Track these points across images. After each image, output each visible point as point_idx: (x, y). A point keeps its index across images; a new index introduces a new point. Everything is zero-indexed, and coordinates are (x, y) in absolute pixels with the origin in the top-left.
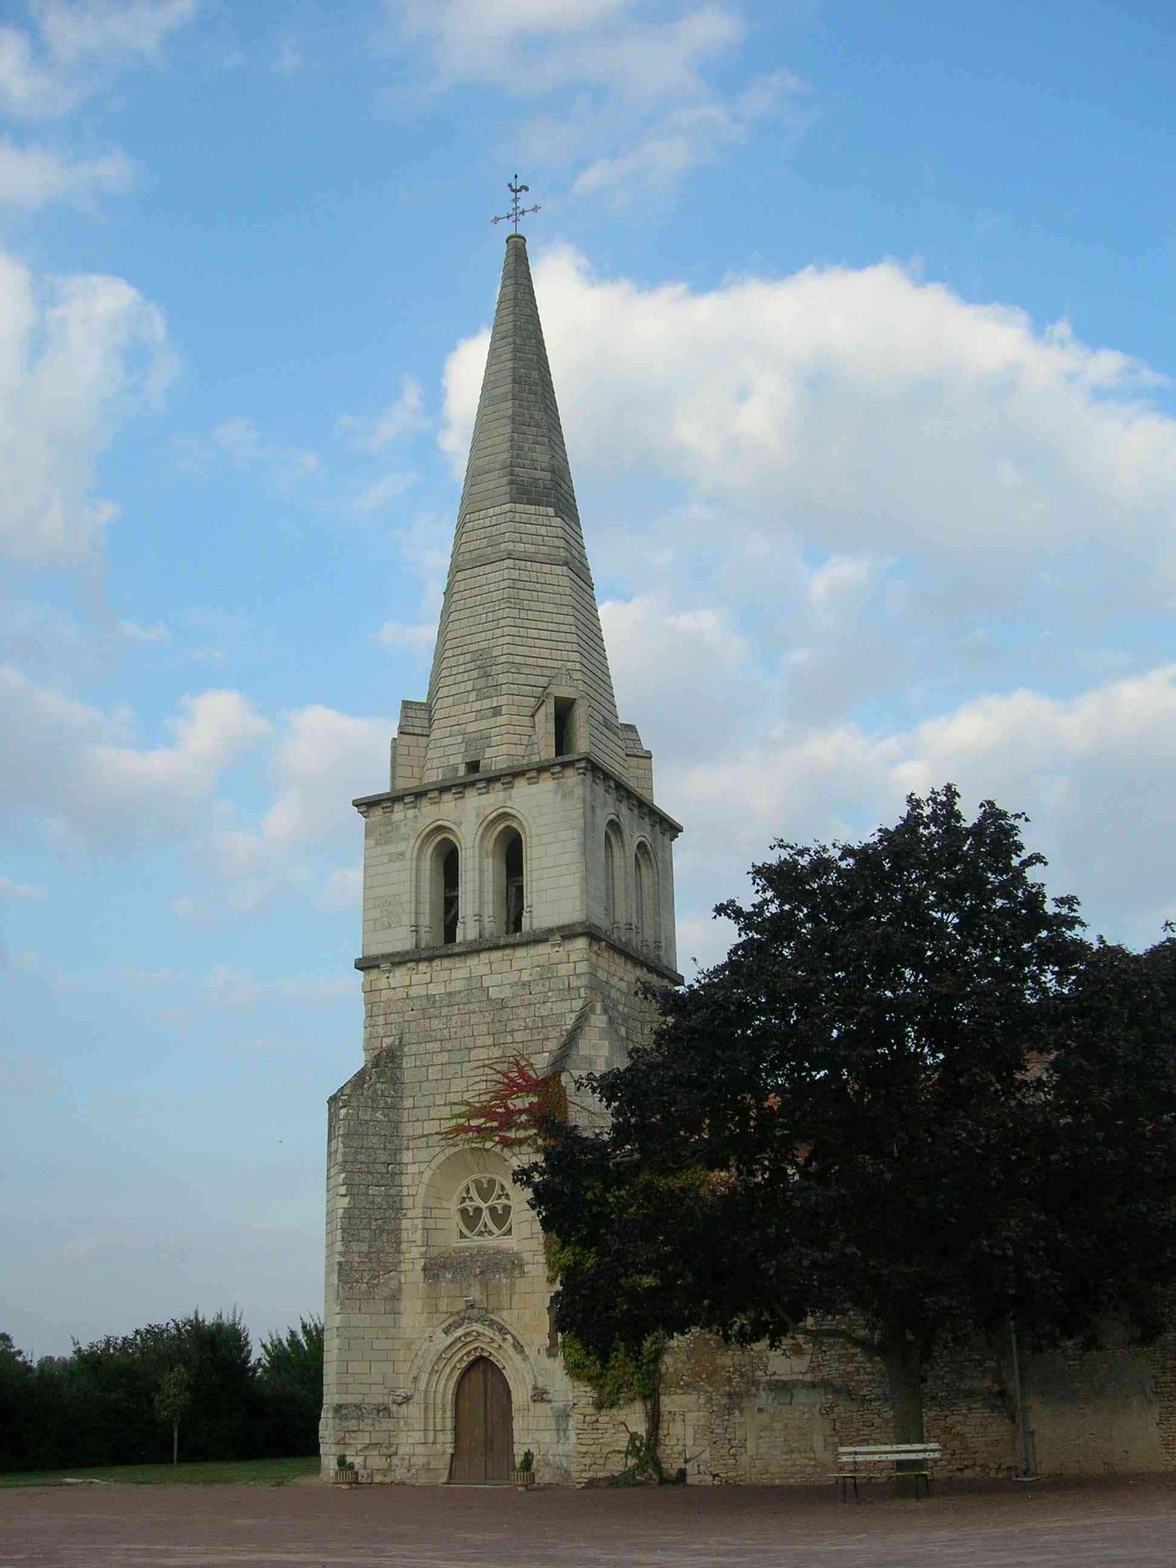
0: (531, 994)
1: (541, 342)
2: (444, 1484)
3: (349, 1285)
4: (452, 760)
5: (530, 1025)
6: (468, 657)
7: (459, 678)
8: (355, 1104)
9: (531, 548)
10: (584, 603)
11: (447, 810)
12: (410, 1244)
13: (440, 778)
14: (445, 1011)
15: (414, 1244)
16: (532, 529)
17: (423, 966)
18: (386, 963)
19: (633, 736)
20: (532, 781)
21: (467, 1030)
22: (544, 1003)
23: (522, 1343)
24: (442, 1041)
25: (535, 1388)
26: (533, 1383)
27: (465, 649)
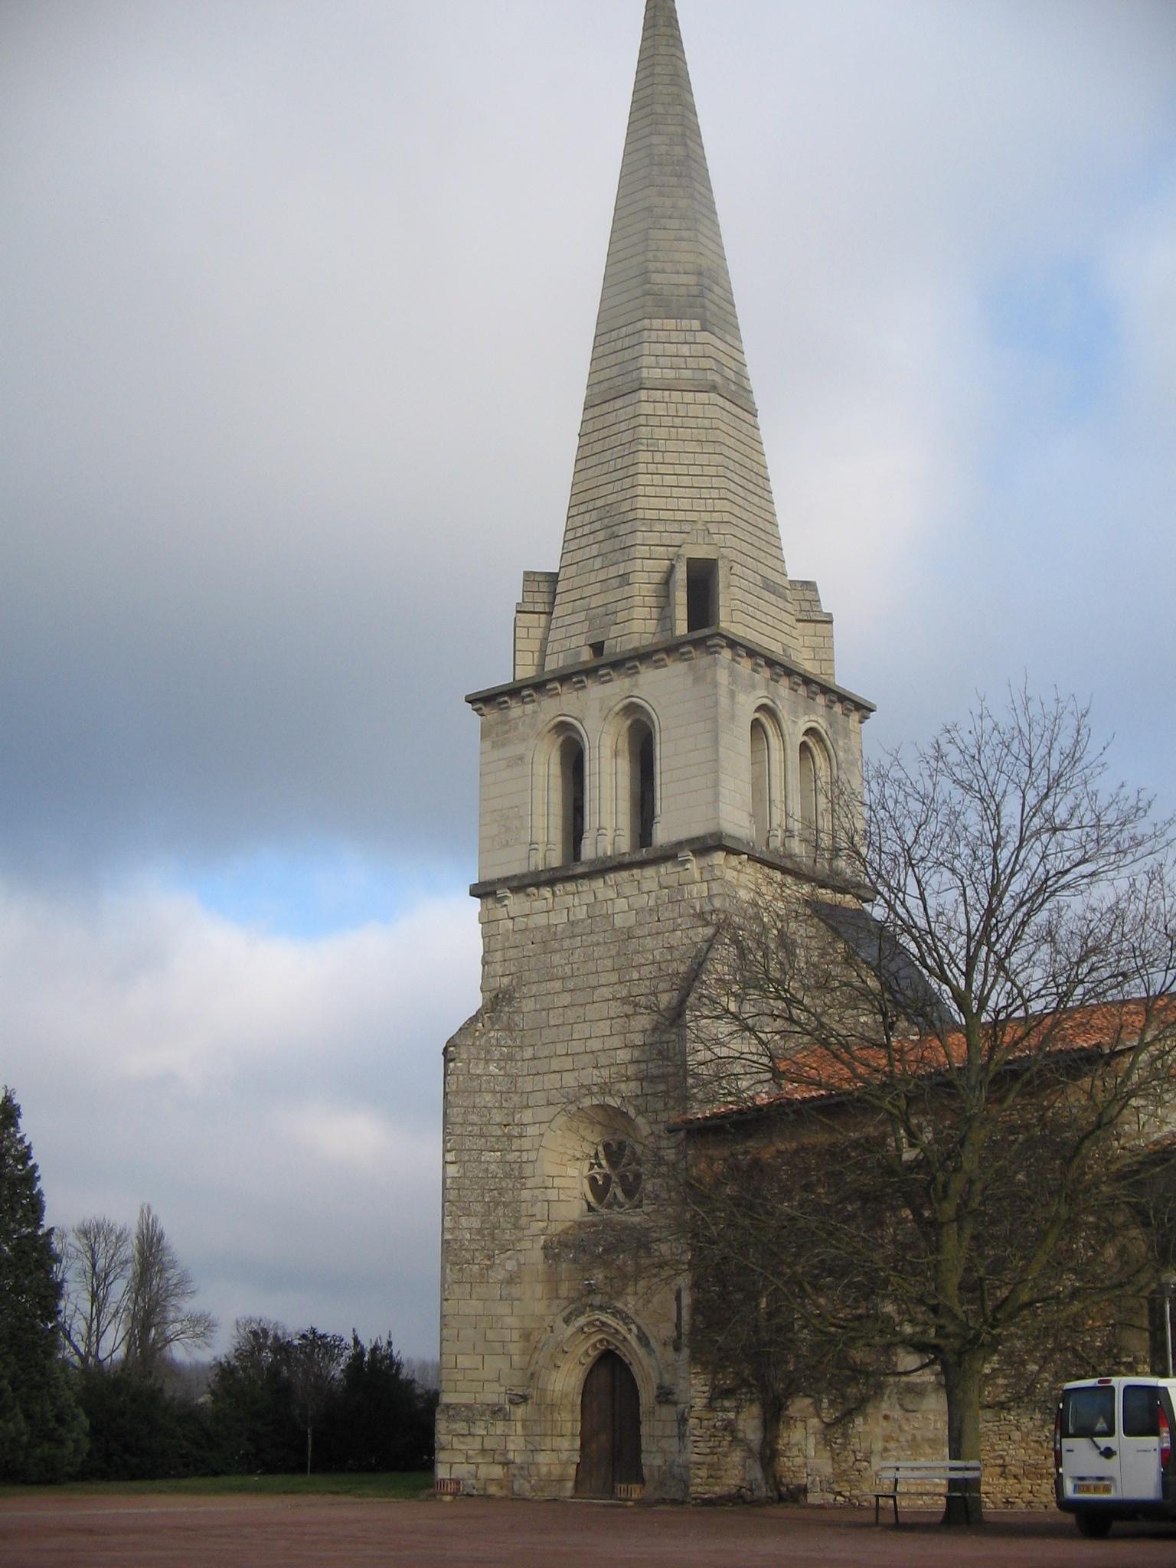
0: (659, 920)
1: (691, 108)
2: (572, 1498)
3: (458, 1267)
4: (574, 642)
5: (658, 958)
6: (594, 515)
7: (584, 541)
8: (464, 1056)
9: (670, 374)
10: (742, 437)
11: (565, 704)
12: (530, 1219)
13: (560, 665)
14: (566, 943)
15: (534, 1218)
16: (671, 349)
17: (546, 892)
18: (504, 888)
19: (809, 595)
20: (659, 665)
21: (591, 966)
22: (674, 930)
23: (648, 1333)
24: (563, 979)
25: (660, 1387)
26: (658, 1381)
27: (591, 506)
